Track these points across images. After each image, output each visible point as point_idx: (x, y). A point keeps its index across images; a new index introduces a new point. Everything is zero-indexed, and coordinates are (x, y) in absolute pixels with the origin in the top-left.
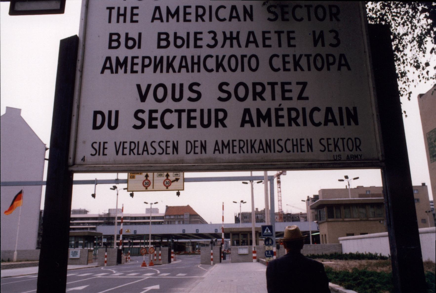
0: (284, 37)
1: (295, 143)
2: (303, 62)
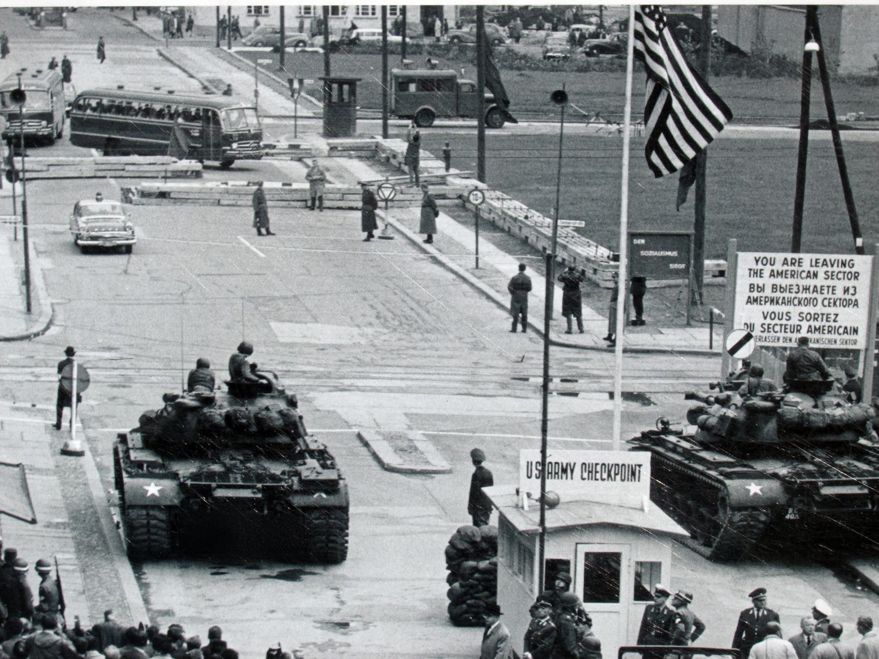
0: (831, 289)
2: (838, 303)
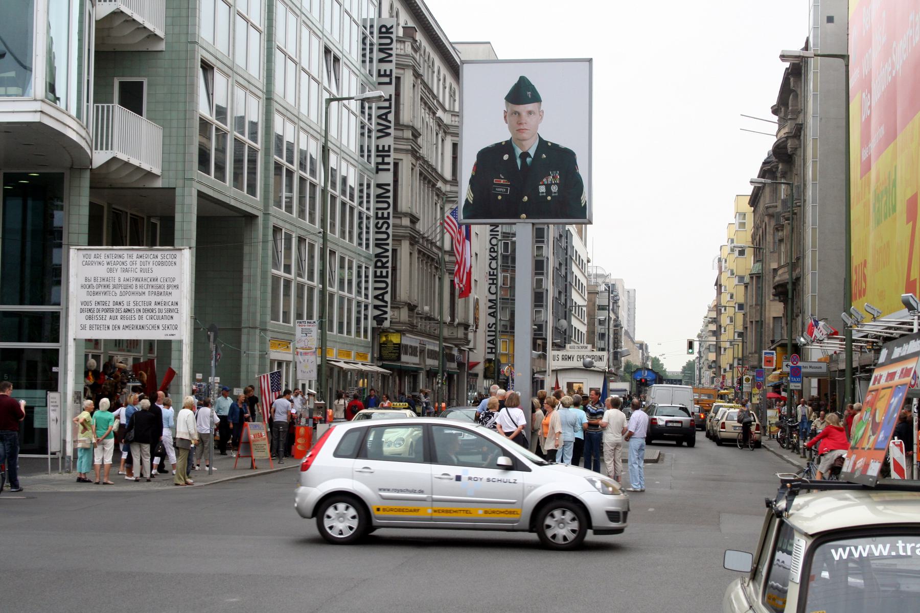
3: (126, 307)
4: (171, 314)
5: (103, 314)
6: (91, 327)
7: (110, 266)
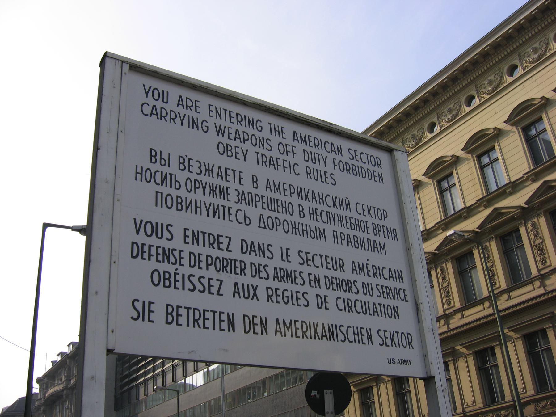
1: (356, 332)
3: (277, 262)
4: (393, 303)
5: (211, 273)
6: (172, 315)
7: (225, 140)
